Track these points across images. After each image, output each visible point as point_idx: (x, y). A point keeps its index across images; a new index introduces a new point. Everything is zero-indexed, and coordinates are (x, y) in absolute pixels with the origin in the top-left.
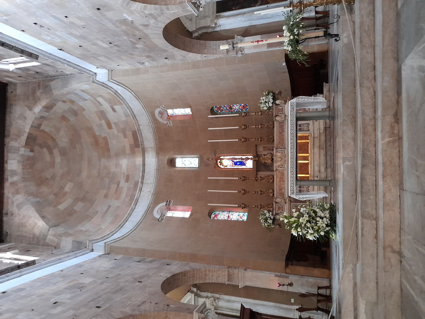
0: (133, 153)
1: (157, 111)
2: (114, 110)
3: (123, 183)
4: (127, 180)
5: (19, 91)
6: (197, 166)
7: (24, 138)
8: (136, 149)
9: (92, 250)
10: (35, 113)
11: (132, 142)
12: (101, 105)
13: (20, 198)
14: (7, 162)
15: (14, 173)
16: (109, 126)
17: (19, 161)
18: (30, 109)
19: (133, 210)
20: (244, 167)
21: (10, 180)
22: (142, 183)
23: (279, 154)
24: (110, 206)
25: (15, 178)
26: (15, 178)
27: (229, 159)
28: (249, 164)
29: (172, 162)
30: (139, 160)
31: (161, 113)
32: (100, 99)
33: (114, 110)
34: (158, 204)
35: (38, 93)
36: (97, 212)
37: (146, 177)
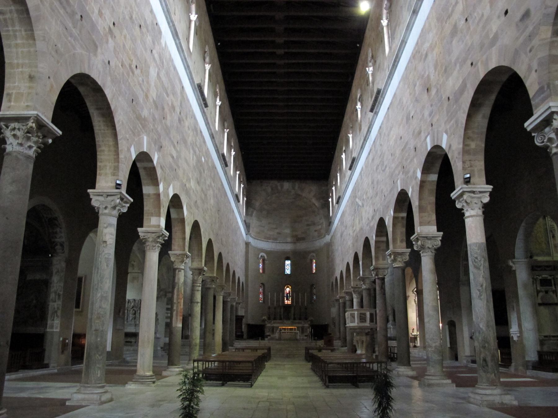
0: (293, 236)
1: (314, 255)
2: (316, 231)
3: (277, 231)
4: (279, 233)
5: (323, 188)
6: (286, 273)
7: (299, 192)
8: (295, 238)
9: (246, 235)
10: (312, 199)
11: (299, 236)
12: (318, 225)
13: (269, 190)
14: (288, 182)
15: (282, 187)
16: (308, 225)
17: (288, 189)
18: (314, 196)
19: (263, 241)
20: (285, 299)
21: (278, 184)
22: (277, 242)
23: (289, 322)
24: (264, 227)
25: (279, 188)
26: (279, 188)
27: (289, 292)
28: (288, 302)
29: (288, 259)
30: (289, 240)
31: (314, 256)
32: (320, 227)
33: (316, 231)
34: (266, 254)
35: (321, 201)
36: (261, 221)
37: (279, 244)
